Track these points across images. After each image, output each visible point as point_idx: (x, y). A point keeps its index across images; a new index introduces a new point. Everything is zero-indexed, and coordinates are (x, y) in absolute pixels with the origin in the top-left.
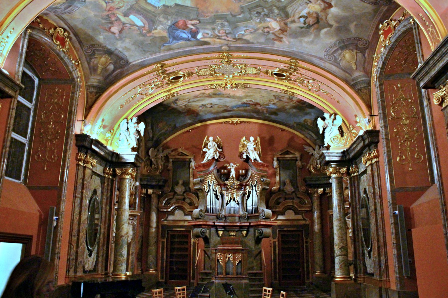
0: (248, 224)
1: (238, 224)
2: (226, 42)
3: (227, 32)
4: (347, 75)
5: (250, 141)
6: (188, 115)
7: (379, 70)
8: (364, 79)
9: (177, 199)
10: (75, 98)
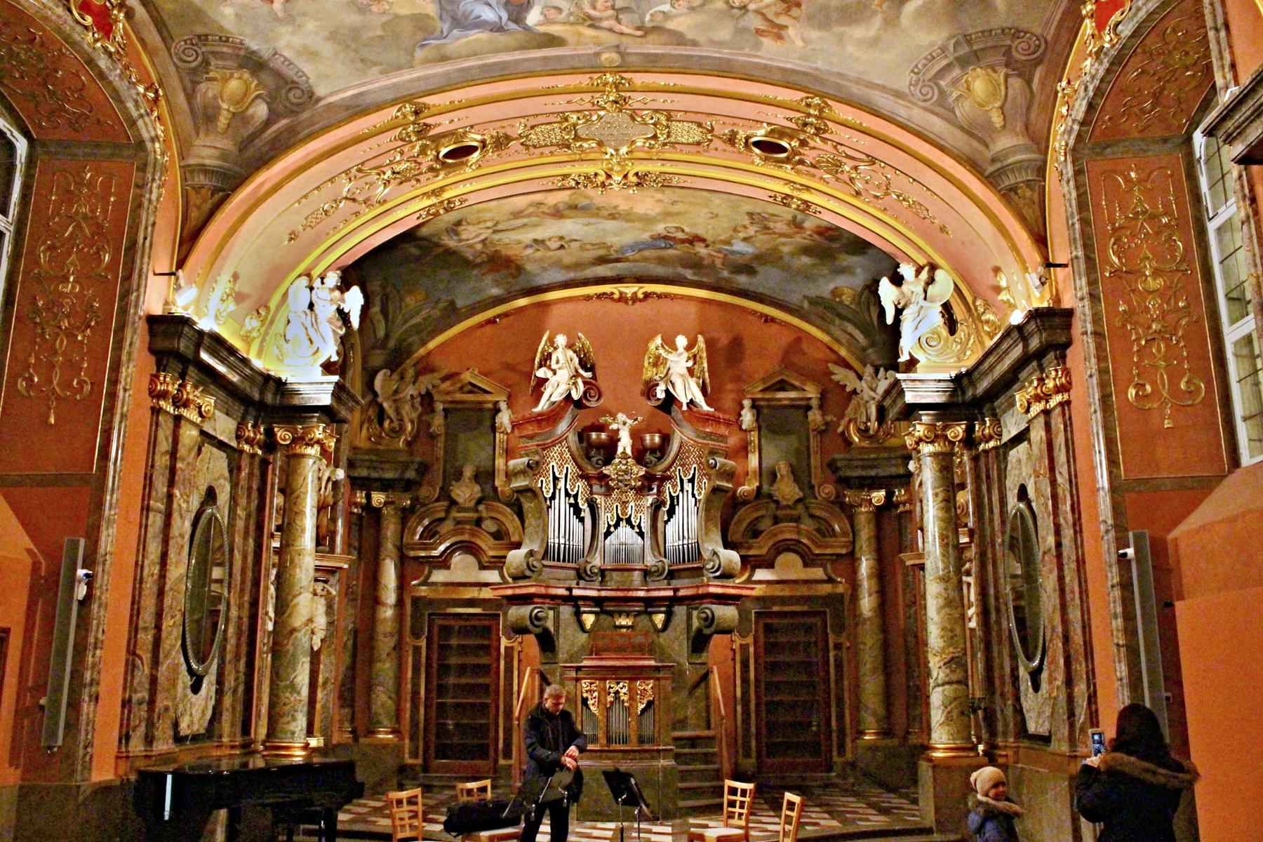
0: (670, 593)
1: (641, 594)
2: (612, 39)
4: (975, 143)
5: (676, 349)
6: (491, 270)
7: (1076, 127)
8: (1024, 157)
9: (458, 522)
10: (146, 203)
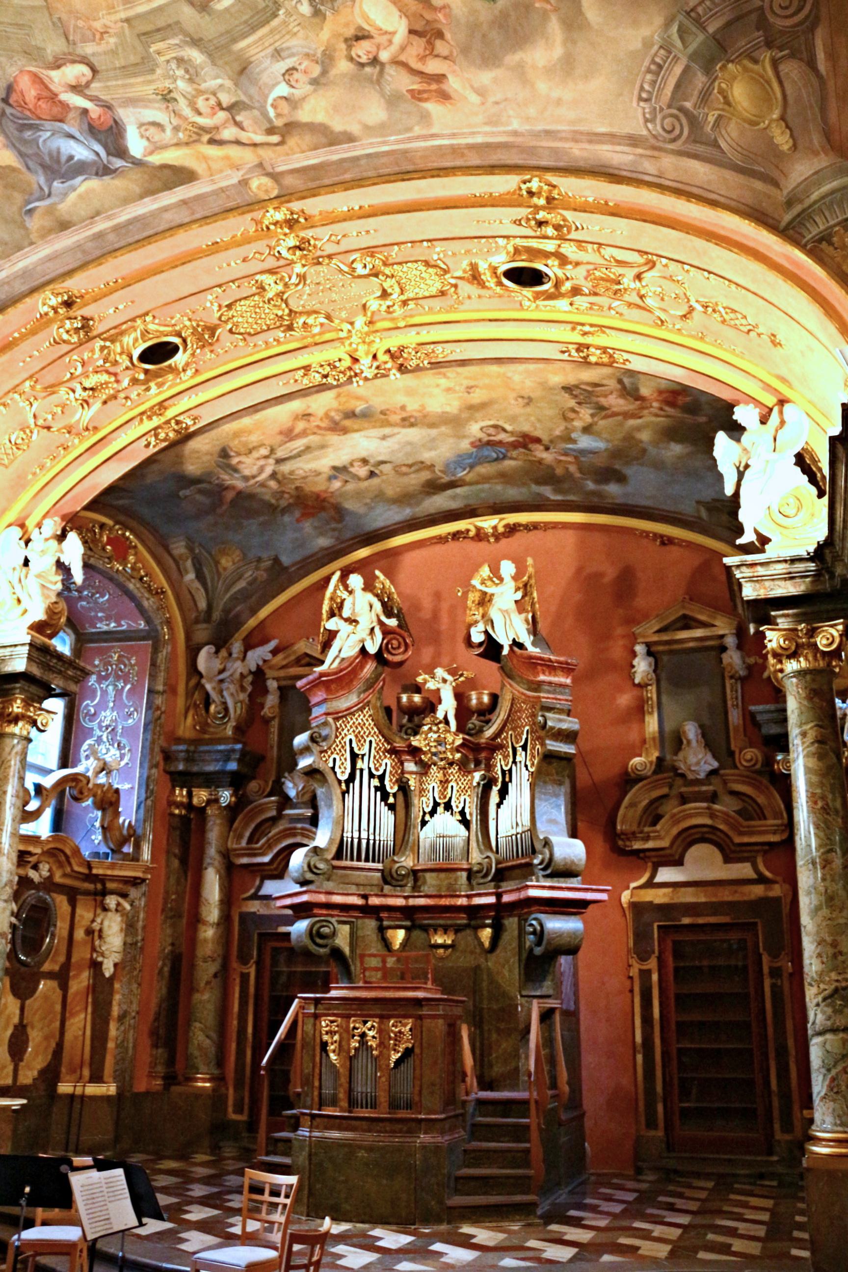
0: (492, 900)
3: (226, 99)
4: (758, 185)
6: (305, 515)
8: (835, 184)
